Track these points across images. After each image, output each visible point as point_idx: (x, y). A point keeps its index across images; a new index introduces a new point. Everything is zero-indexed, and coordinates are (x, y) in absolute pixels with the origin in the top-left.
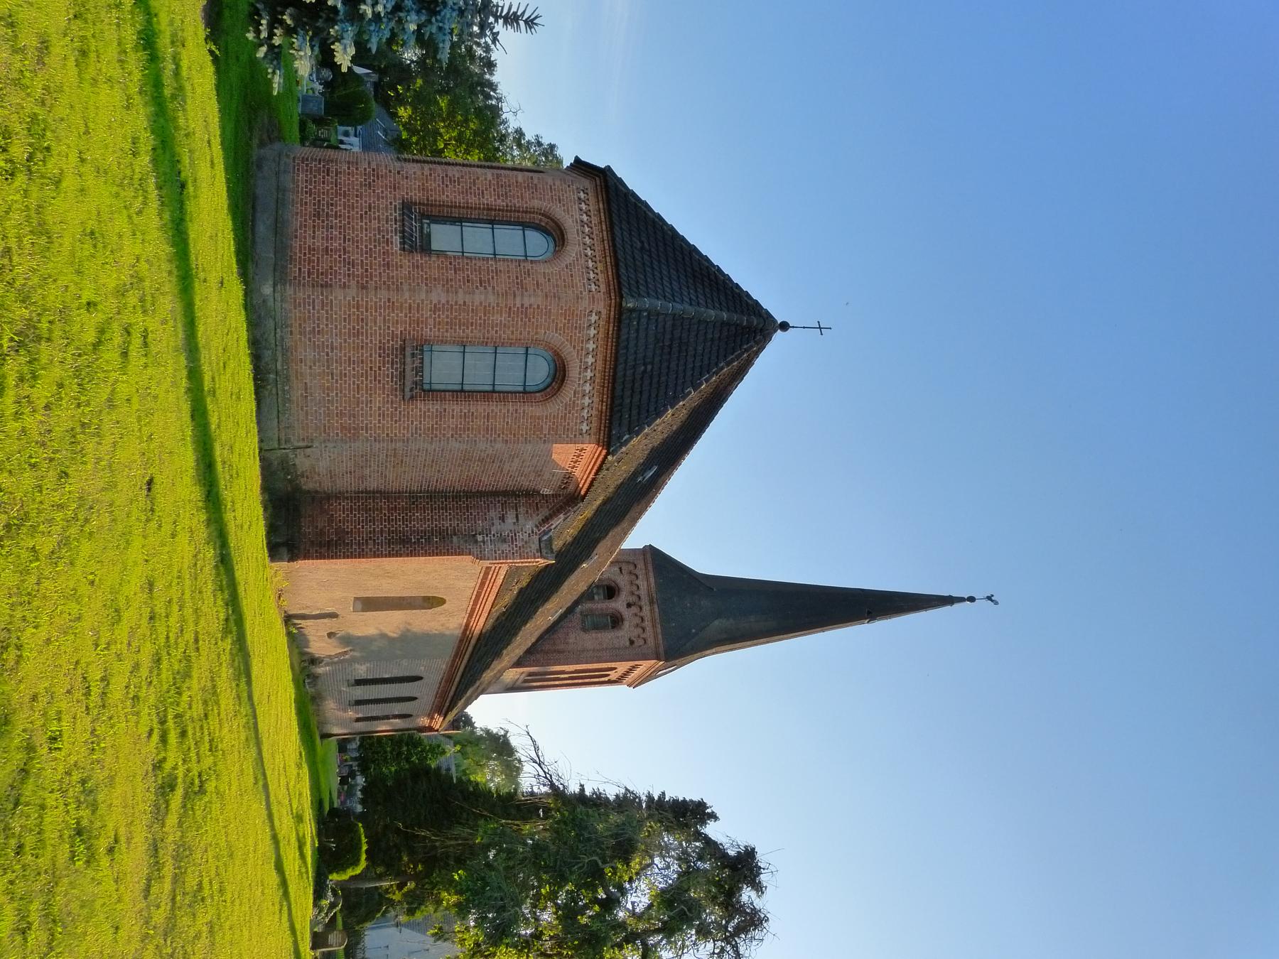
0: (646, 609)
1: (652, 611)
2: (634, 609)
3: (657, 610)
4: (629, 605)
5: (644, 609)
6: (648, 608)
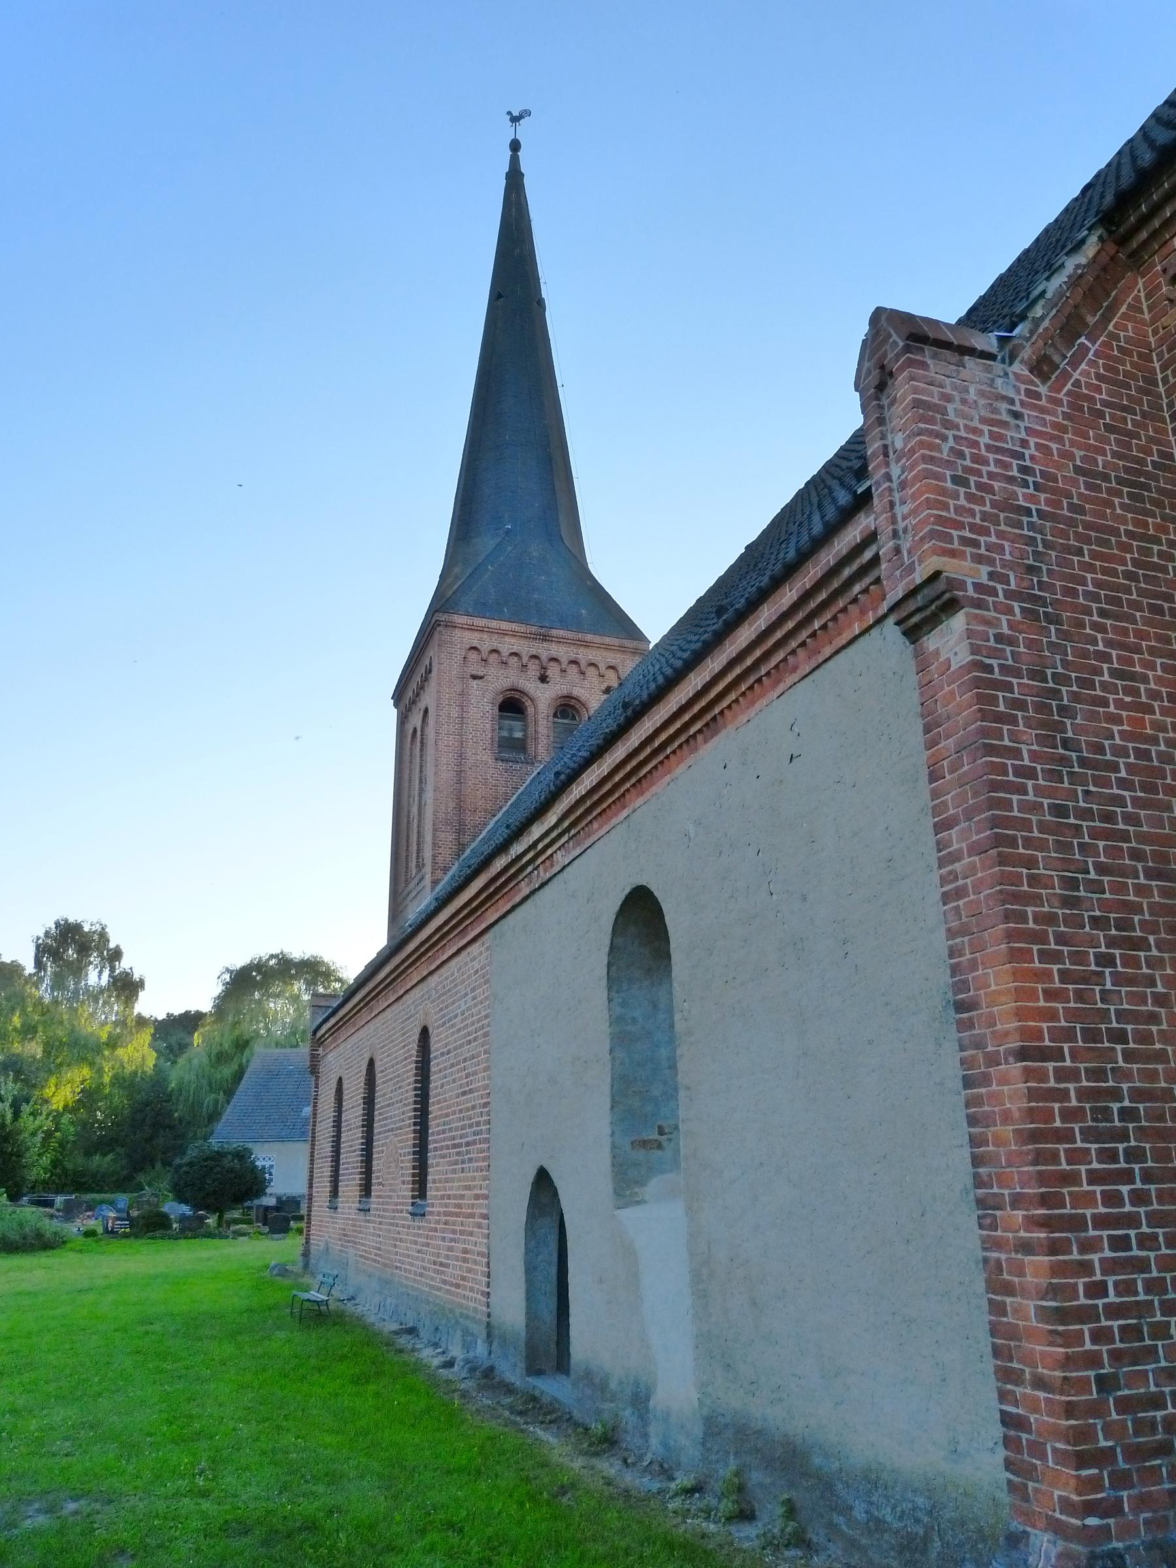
0: (556, 650)
1: (560, 641)
2: (553, 671)
3: (561, 633)
4: (543, 679)
5: (554, 654)
6: (554, 646)
